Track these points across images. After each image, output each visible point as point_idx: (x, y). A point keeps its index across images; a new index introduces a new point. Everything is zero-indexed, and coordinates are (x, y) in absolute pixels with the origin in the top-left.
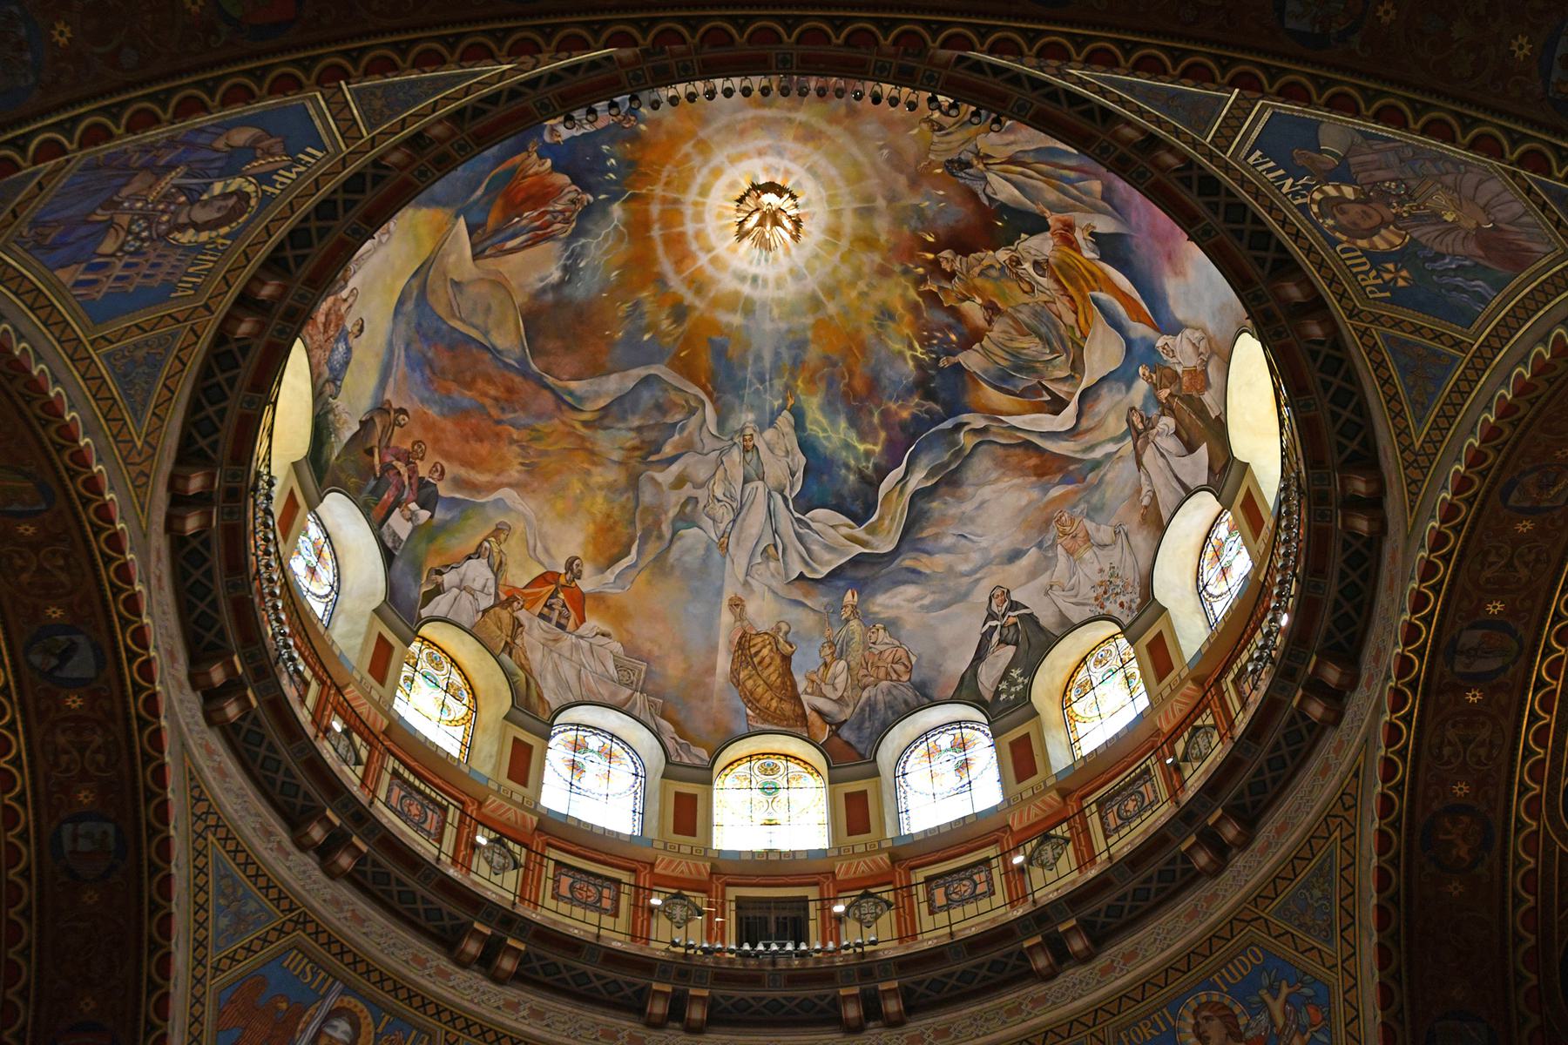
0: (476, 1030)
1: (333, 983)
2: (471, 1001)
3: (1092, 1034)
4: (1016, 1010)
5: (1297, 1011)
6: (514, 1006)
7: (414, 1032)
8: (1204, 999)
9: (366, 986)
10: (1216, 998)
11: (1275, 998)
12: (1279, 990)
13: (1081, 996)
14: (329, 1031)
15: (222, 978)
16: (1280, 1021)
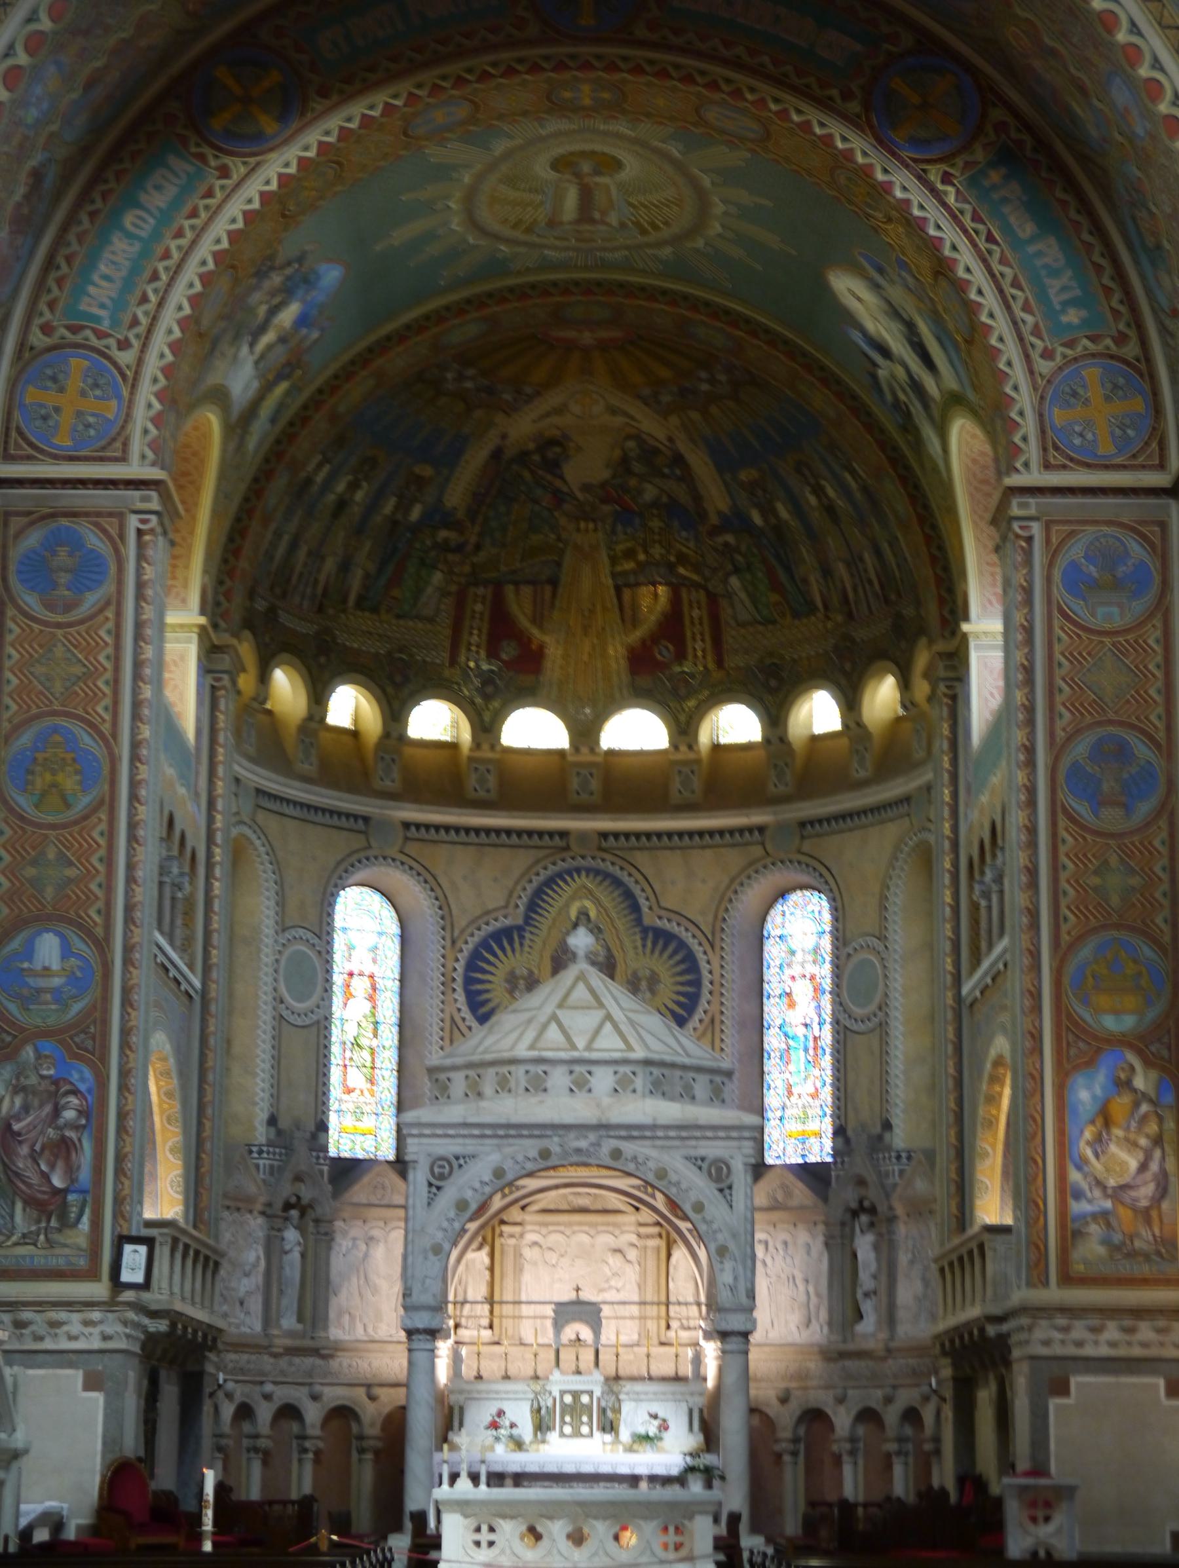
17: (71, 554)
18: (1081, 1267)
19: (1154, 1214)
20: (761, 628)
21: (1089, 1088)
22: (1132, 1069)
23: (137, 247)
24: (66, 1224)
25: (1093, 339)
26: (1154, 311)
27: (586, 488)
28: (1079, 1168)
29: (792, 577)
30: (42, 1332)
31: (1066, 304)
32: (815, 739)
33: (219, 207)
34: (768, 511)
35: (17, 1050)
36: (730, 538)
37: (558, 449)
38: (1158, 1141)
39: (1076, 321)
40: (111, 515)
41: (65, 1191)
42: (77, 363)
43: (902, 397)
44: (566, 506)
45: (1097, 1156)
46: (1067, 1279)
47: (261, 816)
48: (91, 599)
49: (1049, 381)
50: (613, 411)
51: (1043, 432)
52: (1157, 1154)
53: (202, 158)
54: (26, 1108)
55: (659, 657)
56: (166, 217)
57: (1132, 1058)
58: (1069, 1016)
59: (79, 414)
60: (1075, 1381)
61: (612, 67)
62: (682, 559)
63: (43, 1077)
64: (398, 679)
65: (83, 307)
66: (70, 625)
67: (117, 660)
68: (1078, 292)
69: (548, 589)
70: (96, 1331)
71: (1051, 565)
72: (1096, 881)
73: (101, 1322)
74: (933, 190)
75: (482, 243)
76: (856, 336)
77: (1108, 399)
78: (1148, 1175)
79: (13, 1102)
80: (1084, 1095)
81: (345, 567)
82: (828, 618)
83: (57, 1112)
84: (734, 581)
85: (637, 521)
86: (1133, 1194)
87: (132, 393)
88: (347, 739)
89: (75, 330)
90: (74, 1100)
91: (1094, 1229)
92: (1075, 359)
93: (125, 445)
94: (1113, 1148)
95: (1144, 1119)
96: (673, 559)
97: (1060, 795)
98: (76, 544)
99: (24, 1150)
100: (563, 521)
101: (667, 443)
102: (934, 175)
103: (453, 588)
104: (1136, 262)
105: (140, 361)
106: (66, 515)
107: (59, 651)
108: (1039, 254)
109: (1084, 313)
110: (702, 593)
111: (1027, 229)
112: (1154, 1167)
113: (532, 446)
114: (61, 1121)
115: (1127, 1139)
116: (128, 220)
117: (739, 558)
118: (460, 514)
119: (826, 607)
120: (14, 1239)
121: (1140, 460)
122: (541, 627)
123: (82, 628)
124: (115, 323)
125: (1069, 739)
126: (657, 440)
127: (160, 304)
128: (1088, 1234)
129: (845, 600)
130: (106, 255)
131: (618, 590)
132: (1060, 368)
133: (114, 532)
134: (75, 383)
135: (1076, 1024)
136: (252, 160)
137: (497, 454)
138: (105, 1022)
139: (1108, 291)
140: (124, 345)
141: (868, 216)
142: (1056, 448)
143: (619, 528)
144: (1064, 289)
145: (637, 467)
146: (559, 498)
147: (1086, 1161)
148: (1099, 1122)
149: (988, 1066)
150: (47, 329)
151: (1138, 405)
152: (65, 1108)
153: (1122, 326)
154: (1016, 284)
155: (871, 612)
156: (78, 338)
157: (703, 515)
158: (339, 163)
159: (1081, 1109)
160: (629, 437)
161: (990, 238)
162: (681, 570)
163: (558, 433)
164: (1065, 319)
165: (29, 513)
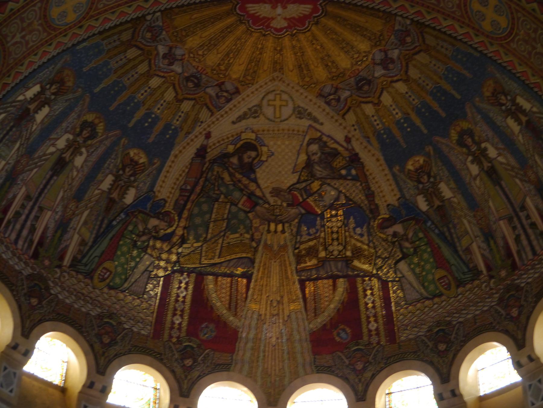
20: (427, 303)
27: (276, 192)
29: (456, 251)
32: (482, 399)
36: (398, 228)
37: (253, 154)
44: (258, 208)
50: (300, 113)
55: (337, 339)
62: (358, 253)
64: (106, 340)
82: (491, 277)
84: (403, 266)
85: (318, 222)
88: (57, 394)
96: (349, 254)
100: (256, 223)
101: (345, 144)
103: (161, 273)
110: (375, 282)
118: (169, 207)
119: (489, 268)
122: (235, 315)
126: (337, 142)
129: (509, 254)
131: (302, 283)
137: (201, 152)
145: (318, 170)
155: (534, 253)
157: (375, 211)
160: (312, 141)
162: (356, 263)
163: (253, 136)
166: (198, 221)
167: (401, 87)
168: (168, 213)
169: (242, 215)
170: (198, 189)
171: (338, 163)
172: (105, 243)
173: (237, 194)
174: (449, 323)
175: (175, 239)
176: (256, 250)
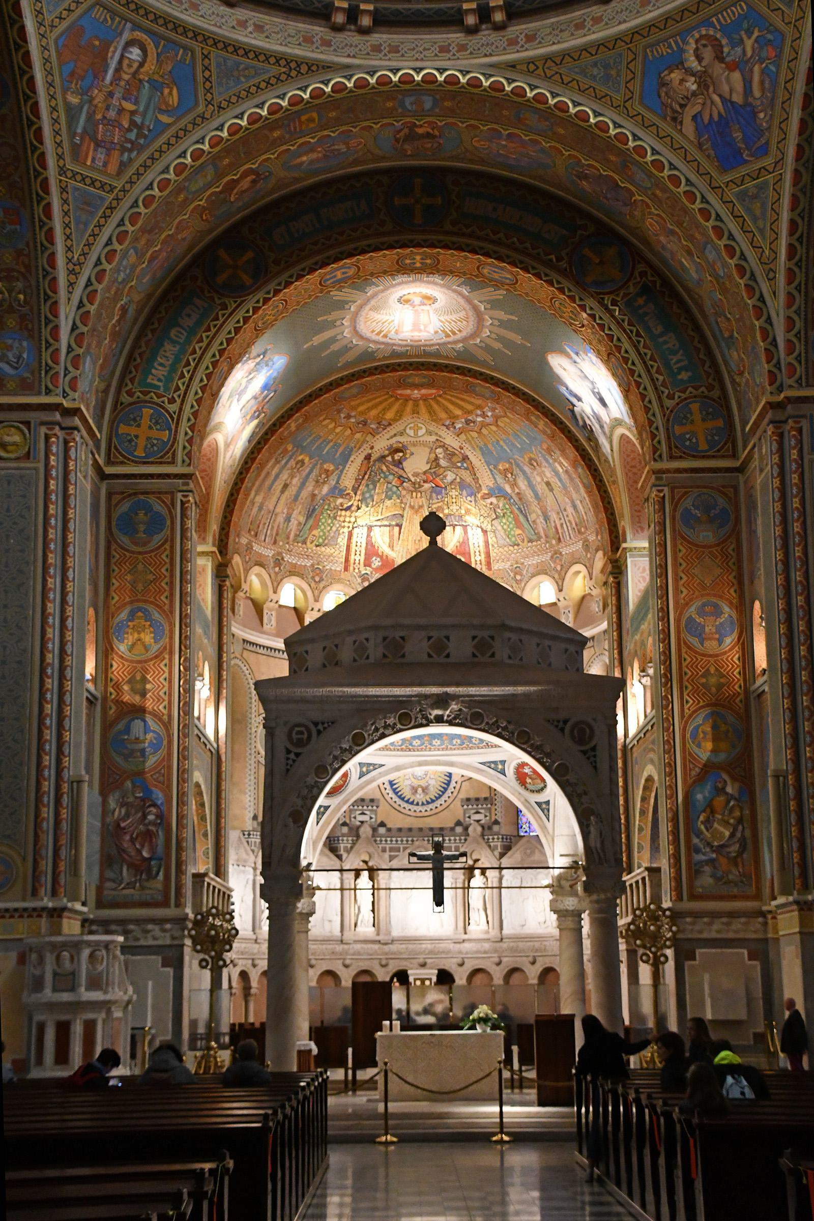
0: (220, 45)
1: (125, 24)
2: (215, 25)
3: (629, 48)
4: (580, 26)
5: (761, 48)
6: (243, 24)
7: (181, 51)
8: (704, 32)
9: (146, 23)
10: (711, 33)
11: (749, 38)
12: (753, 33)
13: (625, 21)
14: (127, 55)
15: (57, 31)
16: (749, 53)
17: (146, 514)
18: (700, 890)
19: (739, 860)
21: (702, 793)
22: (725, 782)
23: (178, 347)
24: (152, 877)
25: (696, 388)
26: (729, 372)
27: (416, 475)
28: (698, 836)
30: (139, 936)
31: (680, 370)
33: (221, 326)
34: (514, 485)
35: (122, 783)
36: (494, 500)
37: (401, 454)
38: (740, 821)
39: (685, 378)
40: (166, 493)
41: (150, 859)
42: (147, 412)
43: (588, 422)
45: (707, 830)
46: (693, 897)
47: (246, 653)
48: (157, 539)
49: (672, 411)
50: (430, 433)
51: (669, 438)
52: (740, 827)
53: (212, 299)
54: (128, 815)
56: (192, 331)
57: (725, 777)
58: (690, 754)
59: (148, 439)
60: (698, 952)
61: (432, 246)
63: (136, 798)
65: (149, 380)
66: (146, 553)
67: (172, 571)
68: (686, 362)
69: (397, 529)
70: (168, 935)
71: (675, 510)
72: (704, 680)
73: (171, 930)
74: (607, 309)
75: (360, 343)
76: (563, 389)
77: (703, 420)
78: (736, 839)
79: (120, 811)
80: (699, 797)
81: (288, 519)
82: (547, 542)
83: (144, 816)
84: (495, 522)
86: (728, 850)
87: (177, 427)
89: (145, 393)
90: (153, 810)
91: (707, 869)
92: (686, 399)
93: (174, 454)
94: (716, 825)
95: (732, 810)
96: (463, 512)
97: (682, 635)
98: (148, 509)
99: (127, 837)
102: (607, 301)
104: (719, 346)
105: (181, 409)
106: (143, 493)
107: (140, 567)
108: (665, 343)
109: (689, 374)
111: (660, 329)
112: (739, 835)
113: (387, 452)
114: (147, 821)
115: (723, 820)
116: (173, 333)
117: (499, 511)
119: (547, 536)
120: (122, 886)
121: (721, 453)
123: (153, 554)
124: (167, 389)
125: (687, 604)
127: (191, 379)
128: (704, 872)
130: (161, 352)
132: (678, 404)
133: (169, 503)
134: (145, 422)
135: (694, 759)
136: (239, 300)
137: (368, 457)
138: (170, 767)
139: (703, 362)
140: (172, 401)
141: (571, 324)
142: (676, 447)
143: (434, 495)
144: (678, 361)
145: (443, 463)
146: (401, 479)
147: (702, 833)
148: (708, 810)
149: (643, 781)
150: (130, 393)
151: (720, 423)
152: (149, 813)
153: (710, 381)
154: (652, 359)
156: (147, 398)
157: (479, 488)
158: (286, 301)
159: (698, 803)
161: (638, 335)
164: (680, 377)
165: (123, 493)
166: (367, 495)
167: (494, 428)
168: (348, 494)
169: (395, 489)
170: (367, 477)
171: (455, 459)
172: (311, 522)
173: (391, 477)
174: (523, 564)
175: (354, 508)
176: (404, 509)
